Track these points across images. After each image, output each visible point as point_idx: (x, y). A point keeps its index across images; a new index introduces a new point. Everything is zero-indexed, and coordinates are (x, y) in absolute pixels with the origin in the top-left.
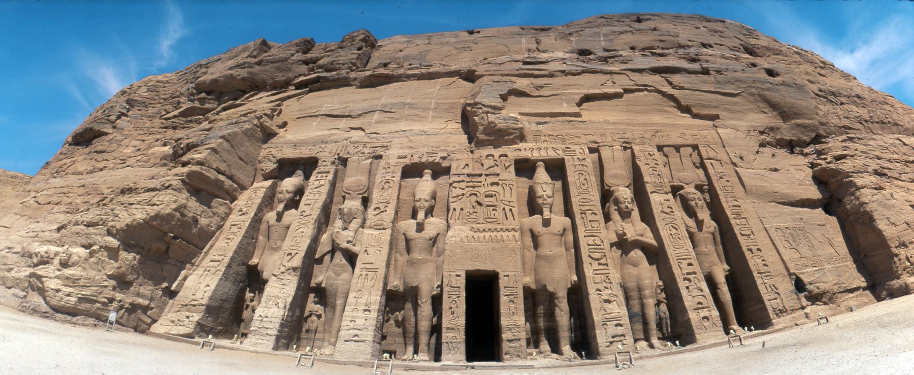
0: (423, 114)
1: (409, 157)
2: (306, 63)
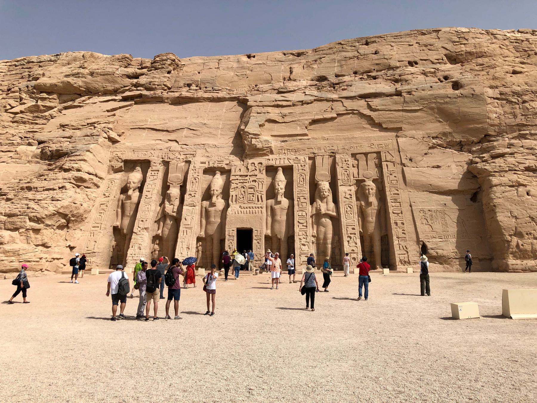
0: (214, 132)
1: (207, 163)
2: (129, 77)
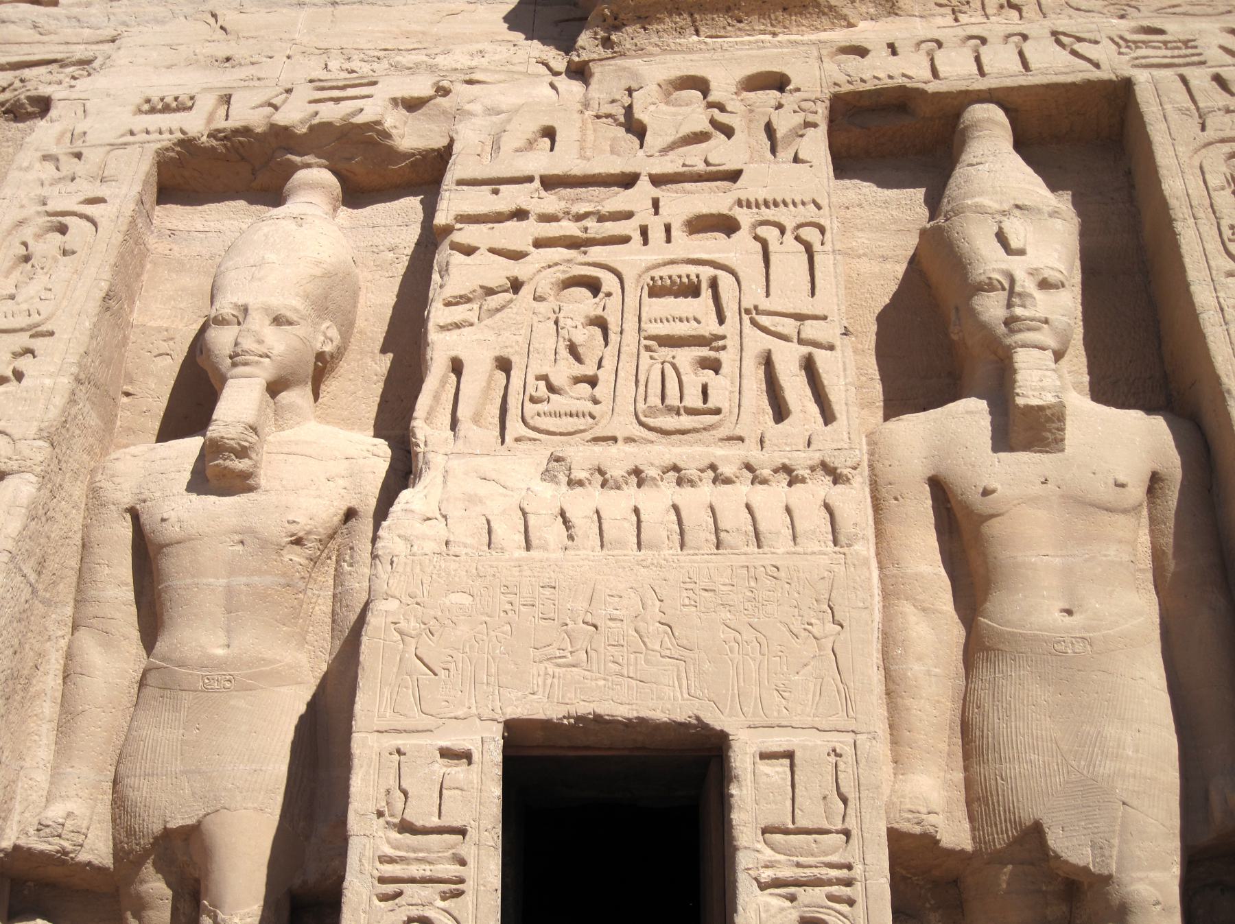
1: (206, 103)
